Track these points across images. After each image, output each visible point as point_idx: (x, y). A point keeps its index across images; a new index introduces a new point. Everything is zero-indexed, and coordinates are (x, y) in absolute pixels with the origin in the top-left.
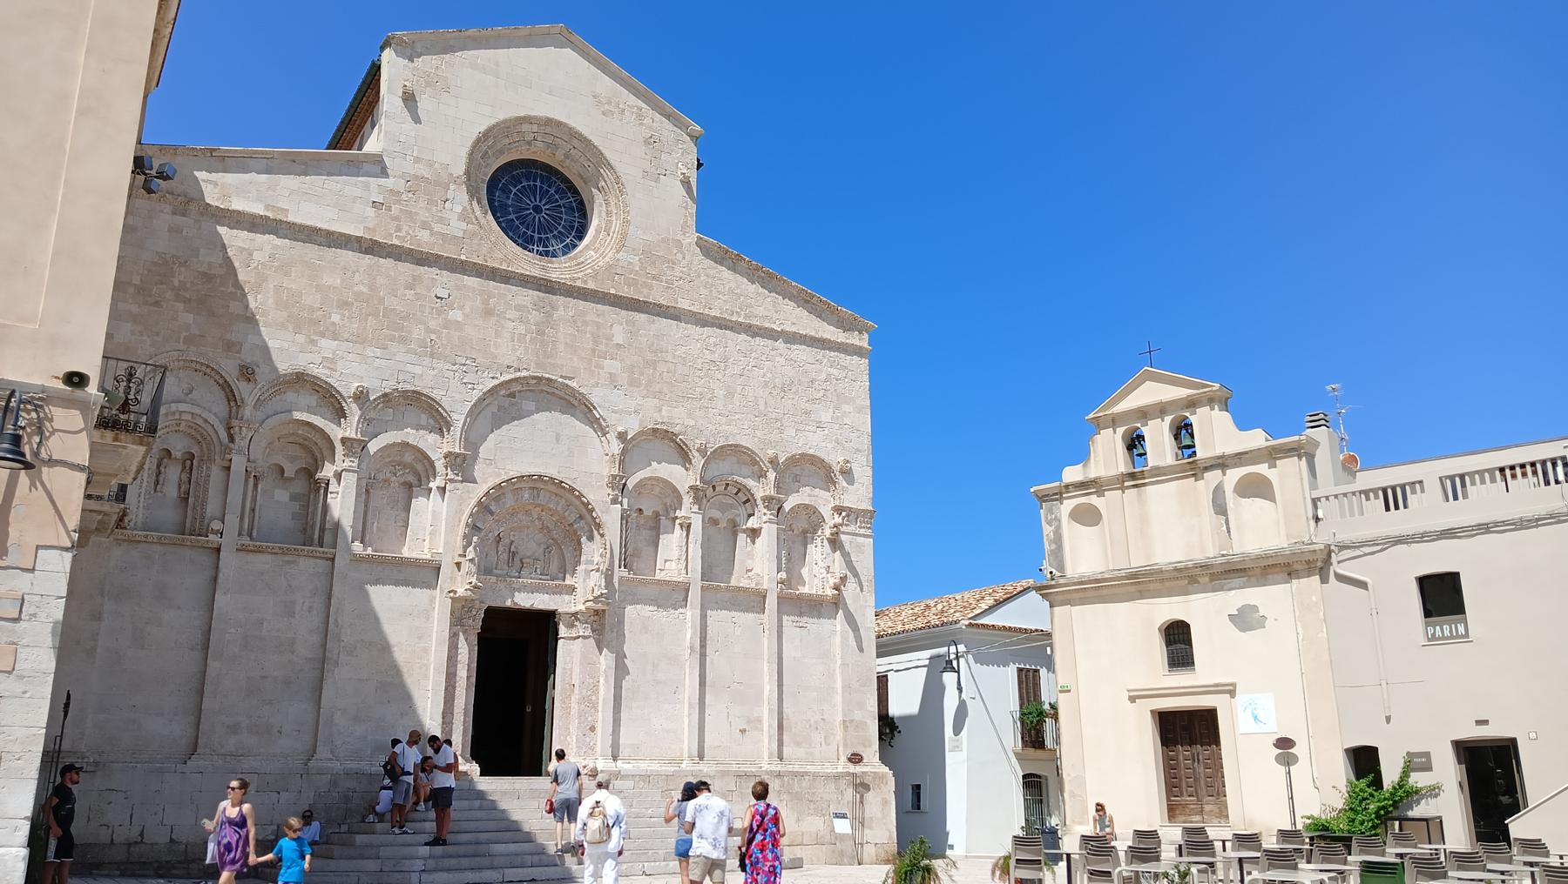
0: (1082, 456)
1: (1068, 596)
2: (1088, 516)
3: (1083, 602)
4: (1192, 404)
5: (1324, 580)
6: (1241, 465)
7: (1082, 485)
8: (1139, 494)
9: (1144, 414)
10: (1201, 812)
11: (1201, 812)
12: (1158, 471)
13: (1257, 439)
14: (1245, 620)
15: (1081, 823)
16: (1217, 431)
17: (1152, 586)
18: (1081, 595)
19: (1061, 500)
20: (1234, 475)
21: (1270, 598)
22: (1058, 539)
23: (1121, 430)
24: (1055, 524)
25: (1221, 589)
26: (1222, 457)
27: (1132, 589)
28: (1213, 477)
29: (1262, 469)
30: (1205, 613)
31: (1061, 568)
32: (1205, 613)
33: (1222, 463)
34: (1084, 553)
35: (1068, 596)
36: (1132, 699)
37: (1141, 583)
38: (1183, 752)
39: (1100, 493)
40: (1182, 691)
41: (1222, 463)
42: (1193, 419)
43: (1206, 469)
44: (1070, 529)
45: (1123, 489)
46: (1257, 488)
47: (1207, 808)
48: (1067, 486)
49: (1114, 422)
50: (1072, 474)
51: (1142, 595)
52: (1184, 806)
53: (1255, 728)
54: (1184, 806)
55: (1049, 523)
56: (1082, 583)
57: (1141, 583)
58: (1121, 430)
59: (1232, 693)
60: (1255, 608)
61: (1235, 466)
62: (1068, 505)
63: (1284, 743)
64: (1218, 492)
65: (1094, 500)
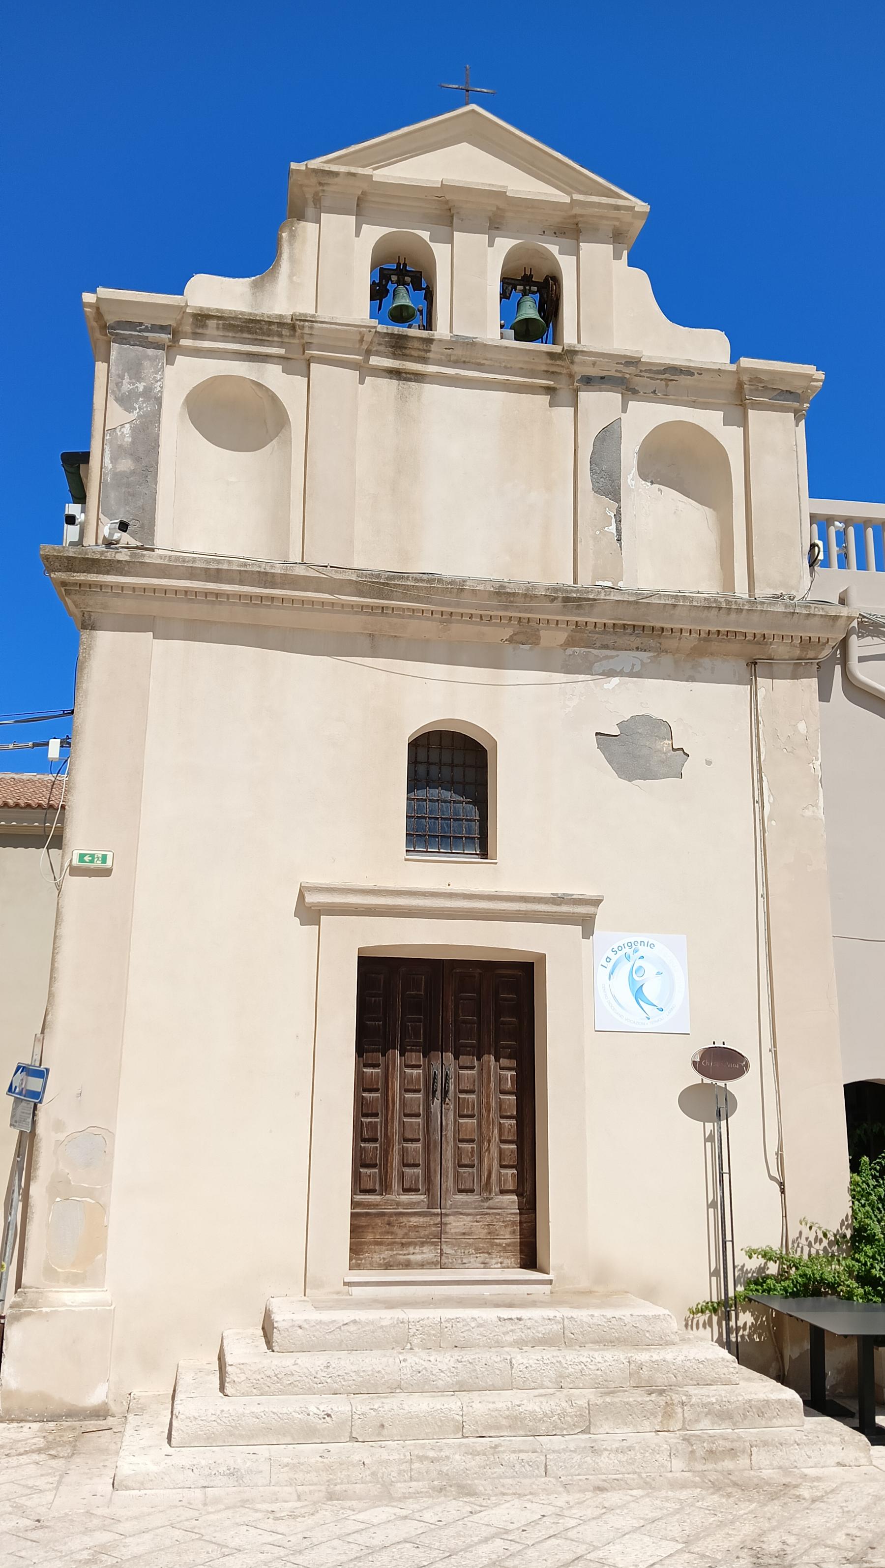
0: (255, 258)
1: (154, 607)
2: (240, 421)
3: (195, 631)
4: (573, 229)
5: (824, 695)
6: (666, 399)
7: (250, 328)
8: (402, 397)
9: (449, 210)
10: (438, 1237)
11: (438, 1237)
12: (466, 354)
13: (709, 348)
14: (636, 751)
15: (75, 1280)
16: (613, 303)
17: (414, 626)
18: (201, 611)
19: (171, 350)
20: (643, 418)
21: (700, 709)
22: (145, 447)
23: (373, 233)
24: (143, 406)
25: (588, 671)
26: (633, 362)
27: (355, 623)
28: (600, 406)
29: (711, 420)
30: (536, 723)
31: (148, 529)
32: (536, 723)
33: (628, 378)
34: (205, 504)
35: (154, 607)
36: (309, 914)
37: (391, 612)
38: (405, 1069)
39: (299, 363)
40: (447, 908)
41: (628, 378)
42: (566, 265)
43: (589, 382)
44: (176, 433)
45: (365, 371)
46: (682, 465)
47: (456, 1224)
48: (202, 318)
49: (363, 205)
50: (208, 292)
51: (375, 645)
52: (391, 1220)
53: (630, 1016)
54: (391, 1220)
55: (126, 402)
56: (216, 575)
57: (391, 612)
58: (373, 233)
59: (587, 925)
60: (660, 728)
61: (654, 396)
62: (182, 376)
63: (722, 1063)
64: (608, 438)
65: (272, 376)
